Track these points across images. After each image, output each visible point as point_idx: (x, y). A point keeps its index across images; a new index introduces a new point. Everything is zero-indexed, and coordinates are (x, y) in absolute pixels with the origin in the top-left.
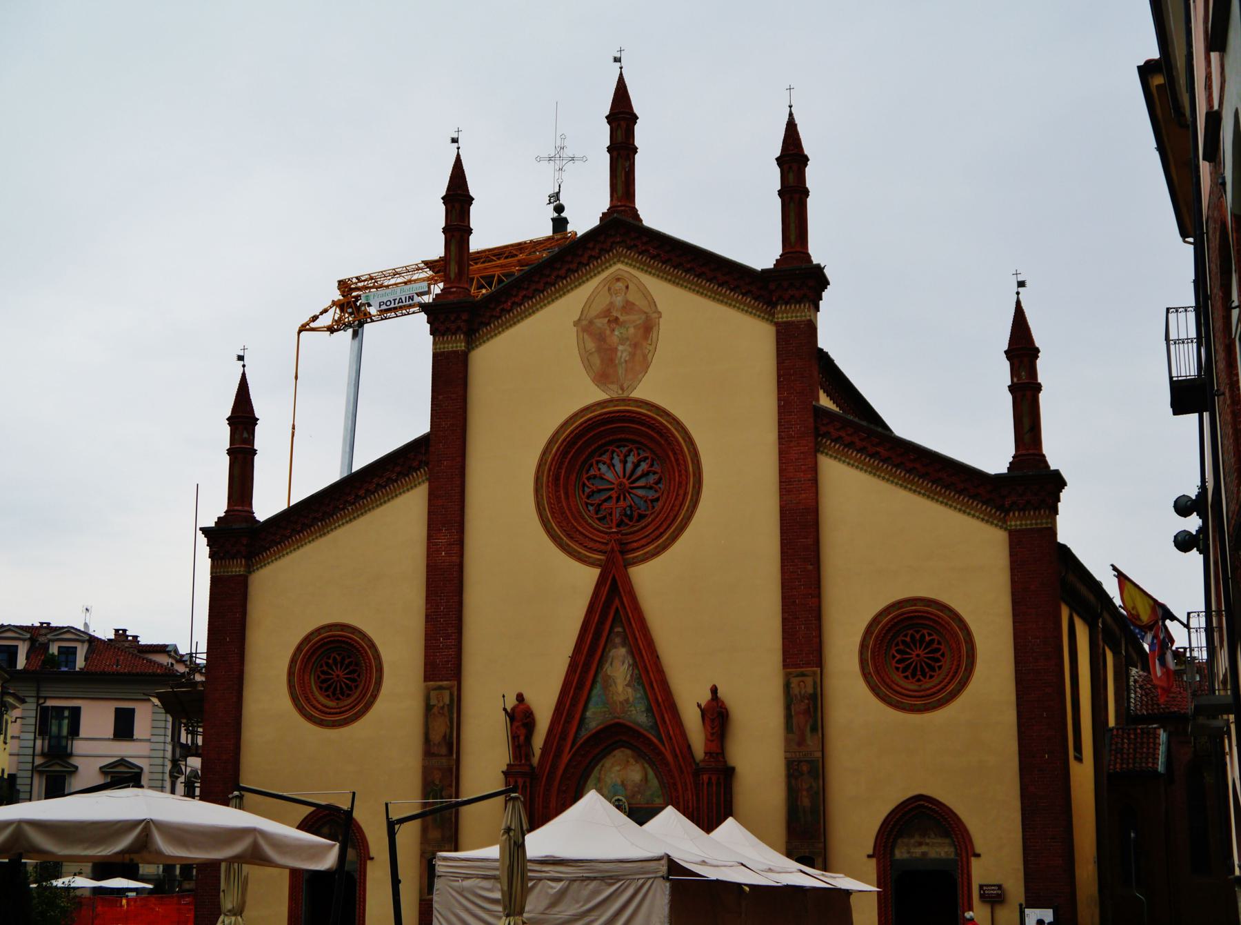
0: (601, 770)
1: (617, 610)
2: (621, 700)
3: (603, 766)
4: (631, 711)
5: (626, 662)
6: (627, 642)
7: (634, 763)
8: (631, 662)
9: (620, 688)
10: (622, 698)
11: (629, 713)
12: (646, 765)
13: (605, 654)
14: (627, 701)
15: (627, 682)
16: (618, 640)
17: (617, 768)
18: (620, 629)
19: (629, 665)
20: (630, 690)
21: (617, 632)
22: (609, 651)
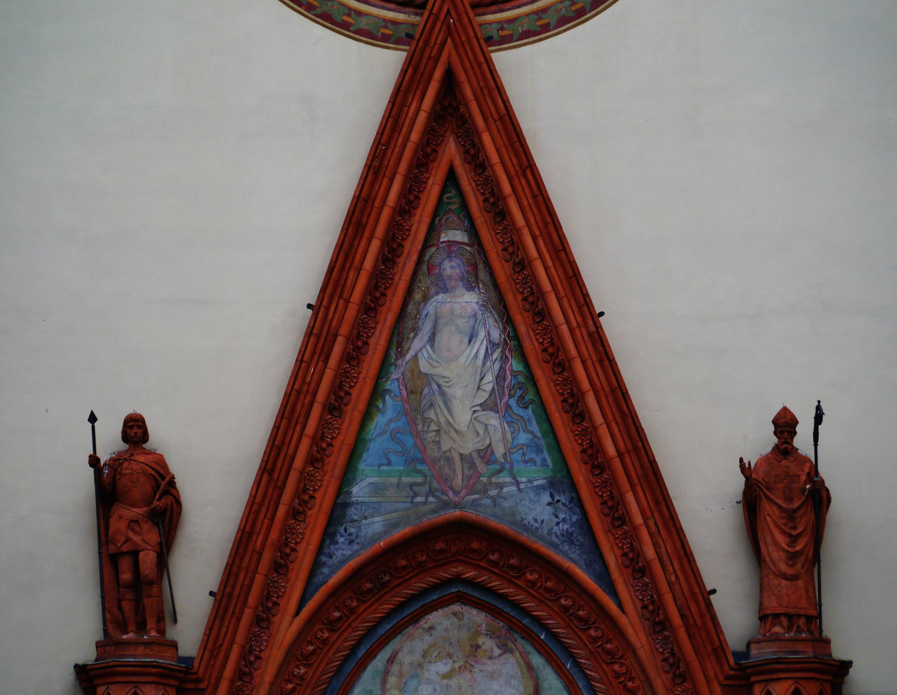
0: (386, 673)
1: (451, 176)
2: (466, 452)
3: (391, 660)
4: (500, 486)
5: (482, 334)
6: (483, 274)
7: (497, 652)
8: (496, 335)
9: (462, 415)
10: (469, 446)
11: (493, 492)
12: (537, 660)
13: (411, 308)
14: (486, 454)
15: (483, 397)
16: (451, 268)
17: (443, 667)
18: (459, 236)
19: (492, 345)
20: (494, 420)
21: (451, 243)
22: (426, 298)
